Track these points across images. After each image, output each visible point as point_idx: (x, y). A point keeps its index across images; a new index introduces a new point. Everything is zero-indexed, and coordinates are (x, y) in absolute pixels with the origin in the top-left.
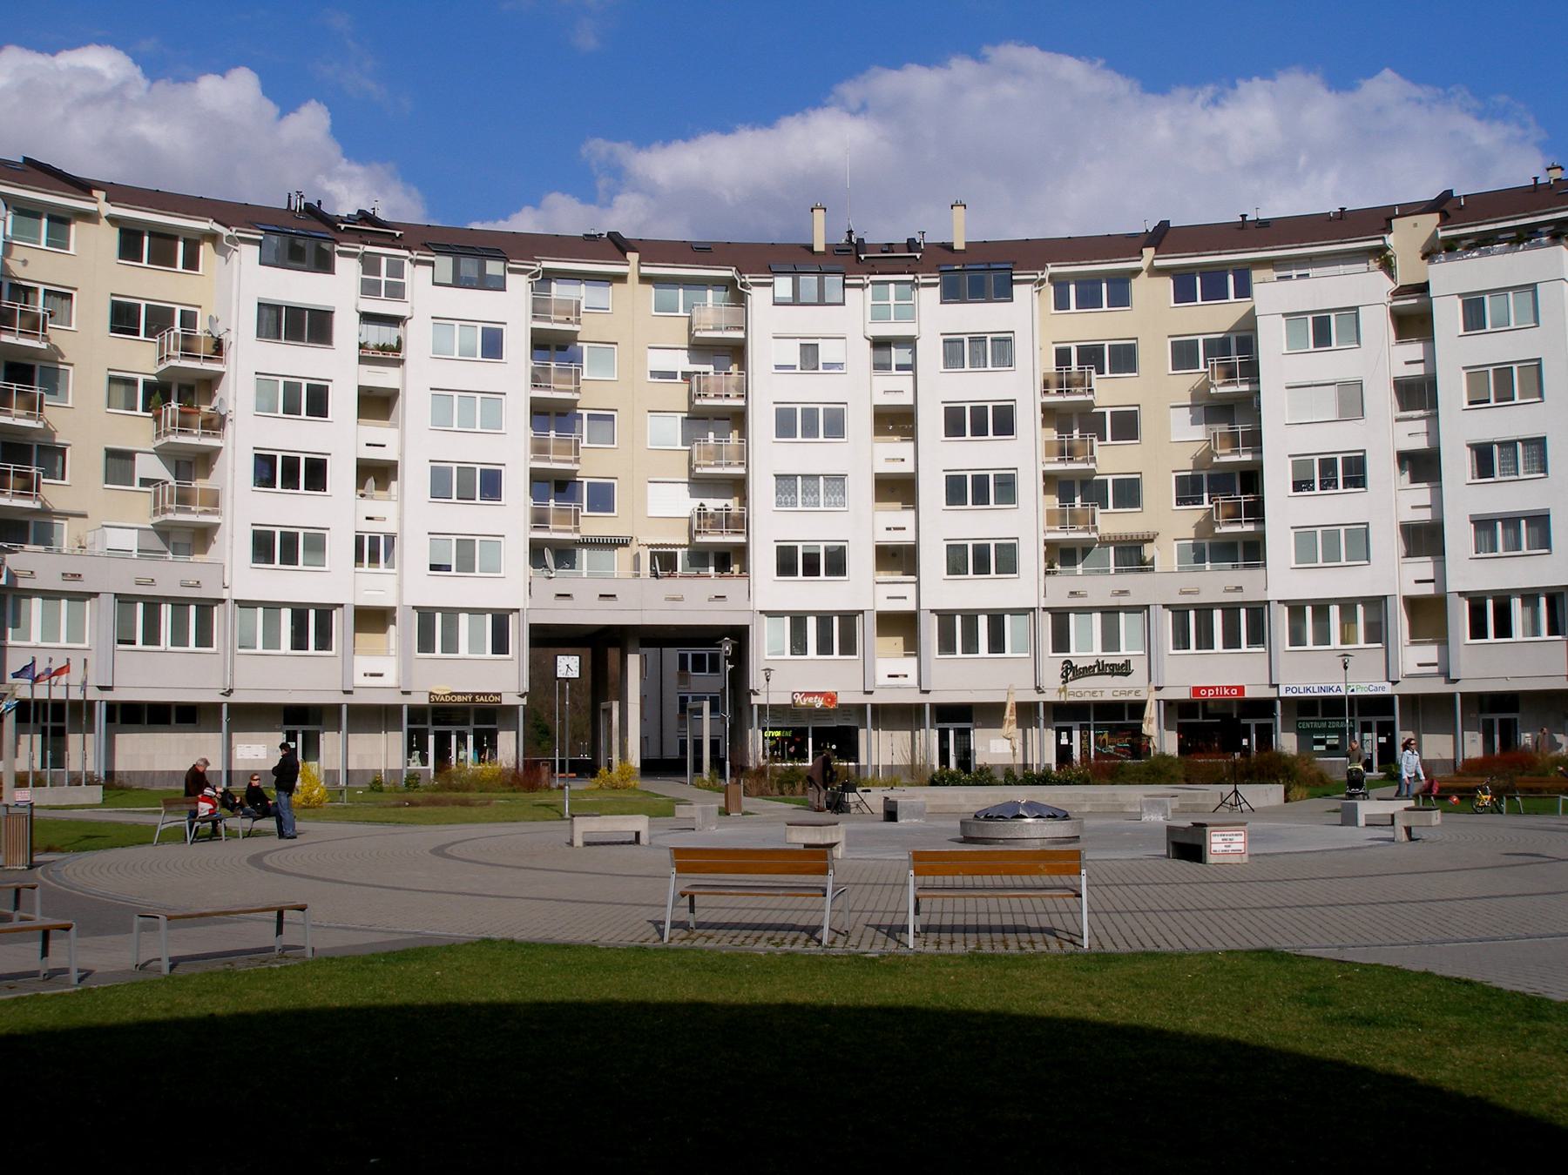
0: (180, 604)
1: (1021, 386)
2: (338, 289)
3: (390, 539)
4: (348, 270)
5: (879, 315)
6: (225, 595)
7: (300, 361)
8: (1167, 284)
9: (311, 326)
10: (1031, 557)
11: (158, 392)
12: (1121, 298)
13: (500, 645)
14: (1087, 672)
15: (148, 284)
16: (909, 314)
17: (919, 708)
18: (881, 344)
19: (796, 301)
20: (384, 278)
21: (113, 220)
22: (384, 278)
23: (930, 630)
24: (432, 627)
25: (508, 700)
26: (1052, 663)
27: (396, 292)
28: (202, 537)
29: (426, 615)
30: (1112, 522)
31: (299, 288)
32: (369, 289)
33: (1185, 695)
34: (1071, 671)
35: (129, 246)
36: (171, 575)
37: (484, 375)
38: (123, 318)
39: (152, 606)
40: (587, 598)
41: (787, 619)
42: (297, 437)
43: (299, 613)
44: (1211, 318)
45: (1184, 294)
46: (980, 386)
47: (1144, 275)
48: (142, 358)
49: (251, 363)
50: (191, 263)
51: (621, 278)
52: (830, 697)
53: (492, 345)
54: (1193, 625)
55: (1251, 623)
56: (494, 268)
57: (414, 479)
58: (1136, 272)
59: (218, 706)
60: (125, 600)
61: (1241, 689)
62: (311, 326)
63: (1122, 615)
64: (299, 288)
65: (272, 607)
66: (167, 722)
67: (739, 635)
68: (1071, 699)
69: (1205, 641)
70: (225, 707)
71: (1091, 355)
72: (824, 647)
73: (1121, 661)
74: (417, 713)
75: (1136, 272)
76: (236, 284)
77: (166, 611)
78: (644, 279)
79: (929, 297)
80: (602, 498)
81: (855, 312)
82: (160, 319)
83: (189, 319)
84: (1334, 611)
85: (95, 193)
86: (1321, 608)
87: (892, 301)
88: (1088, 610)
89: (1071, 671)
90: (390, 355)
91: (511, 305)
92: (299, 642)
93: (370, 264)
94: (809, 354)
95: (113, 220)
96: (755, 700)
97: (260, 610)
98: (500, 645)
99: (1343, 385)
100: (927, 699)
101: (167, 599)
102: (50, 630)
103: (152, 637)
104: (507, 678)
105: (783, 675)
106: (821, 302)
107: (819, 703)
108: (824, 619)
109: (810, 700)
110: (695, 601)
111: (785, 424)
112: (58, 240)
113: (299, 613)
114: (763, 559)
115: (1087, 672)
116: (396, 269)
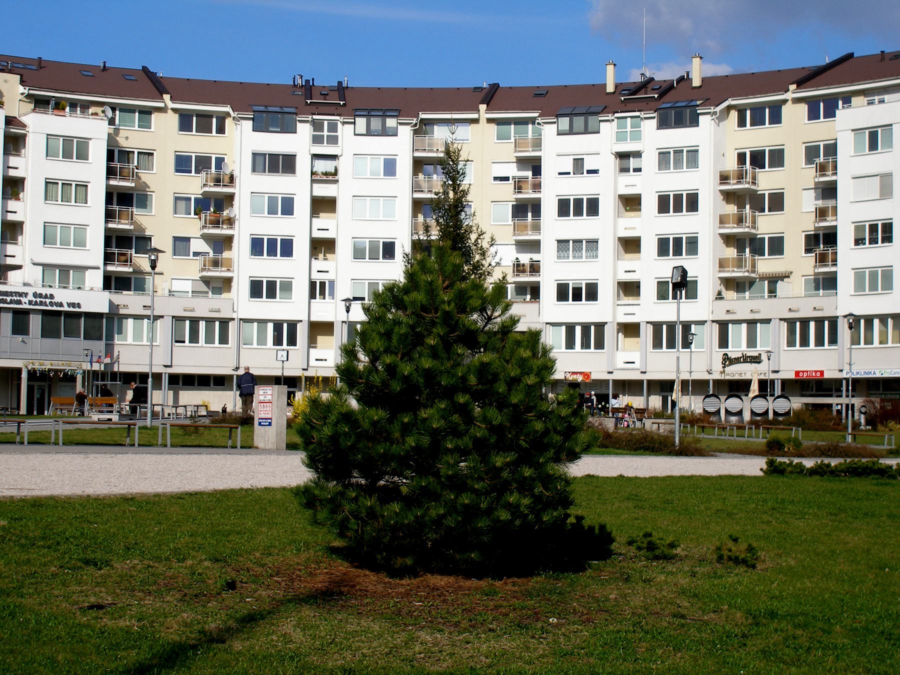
0: (210, 321)
1: (703, 181)
2: (299, 142)
3: (332, 283)
4: (304, 130)
5: (621, 137)
6: (234, 316)
7: (278, 184)
8: (804, 108)
9: (283, 164)
11: (202, 204)
12: (776, 118)
14: (737, 361)
15: (197, 144)
16: (636, 136)
17: (641, 382)
18: (623, 156)
19: (571, 132)
20: (326, 133)
21: (175, 110)
22: (326, 133)
23: (647, 333)
27: (333, 140)
28: (226, 284)
30: (767, 265)
31: (275, 143)
32: (317, 140)
33: (792, 376)
34: (728, 361)
35: (185, 123)
36: (204, 307)
37: (388, 186)
38: (182, 164)
39: (195, 322)
41: (564, 328)
42: (275, 227)
43: (278, 326)
44: (820, 131)
45: (813, 115)
46: (678, 181)
47: (790, 102)
48: (194, 185)
49: (250, 186)
50: (221, 130)
51: (476, 121)
52: (586, 375)
53: (390, 168)
54: (799, 330)
55: (826, 329)
56: (391, 122)
57: (344, 248)
58: (785, 101)
59: (231, 376)
60: (178, 319)
61: (822, 373)
62: (283, 164)
63: (759, 325)
65: (262, 322)
66: (193, 385)
68: (727, 378)
69: (805, 342)
70: (235, 377)
71: (758, 159)
72: (586, 345)
73: (756, 354)
75: (785, 101)
76: (240, 141)
77: (202, 325)
78: (490, 121)
79: (649, 126)
81: (605, 139)
82: (203, 163)
83: (220, 161)
84: (876, 322)
85: (164, 96)
86: (869, 320)
87: (629, 129)
88: (738, 322)
89: (728, 361)
90: (331, 177)
92: (278, 341)
93: (317, 126)
94: (578, 163)
95: (175, 110)
97: (255, 324)
100: (645, 377)
101: (202, 319)
102: (138, 335)
103: (194, 338)
106: (586, 131)
107: (580, 378)
108: (586, 328)
109: (575, 377)
111: (564, 208)
112: (145, 124)
113: (278, 326)
114: (548, 292)
115: (737, 361)
116: (333, 127)
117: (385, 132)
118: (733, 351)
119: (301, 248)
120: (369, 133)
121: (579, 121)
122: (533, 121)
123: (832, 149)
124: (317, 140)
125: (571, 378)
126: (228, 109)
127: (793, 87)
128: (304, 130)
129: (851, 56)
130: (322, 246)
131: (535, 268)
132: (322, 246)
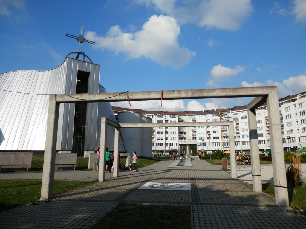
2: (163, 119)
3: (168, 138)
4: (164, 117)
10: (220, 138)
13: (177, 146)
14: (225, 147)
19: (200, 117)
24: (171, 145)
25: (177, 150)
26: (222, 147)
29: (170, 144)
31: (160, 119)
34: (224, 147)
40: (183, 142)
52: (203, 150)
57: (169, 133)
64: (160, 119)
67: (196, 145)
74: (170, 151)
80: (185, 133)
84: (246, 142)
86: (245, 142)
91: (176, 119)
92: (161, 146)
93: (165, 117)
96: (197, 150)
98: (177, 146)
99: (246, 122)
104: (178, 148)
105: (199, 148)
106: (202, 117)
107: (203, 150)
110: (193, 142)
113: (161, 143)
114: (197, 139)
115: (225, 147)
117: (174, 117)
118: (225, 146)
119: (164, 133)
120: (172, 117)
121: (201, 116)
122: (194, 115)
123: (237, 119)
124: (166, 118)
125: (201, 150)
126: (153, 115)
127: (230, 111)
128: (164, 117)
129: (236, 106)
130: (166, 133)
131: (196, 135)
132: (166, 133)
